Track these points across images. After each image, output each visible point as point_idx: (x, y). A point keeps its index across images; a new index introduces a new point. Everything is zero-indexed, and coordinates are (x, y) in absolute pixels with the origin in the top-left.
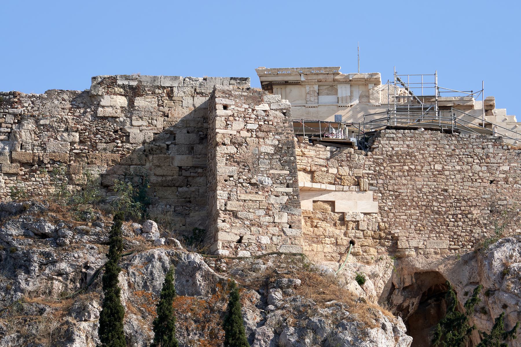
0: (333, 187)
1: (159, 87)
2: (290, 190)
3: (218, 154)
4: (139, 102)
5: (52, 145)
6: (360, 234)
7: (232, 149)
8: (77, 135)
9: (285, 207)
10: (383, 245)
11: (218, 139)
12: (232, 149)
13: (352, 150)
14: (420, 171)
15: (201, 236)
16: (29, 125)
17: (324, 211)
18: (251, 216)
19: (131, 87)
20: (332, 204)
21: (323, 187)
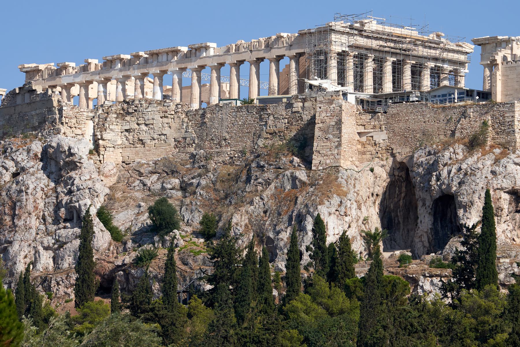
0: (372, 130)
1: (312, 97)
2: (339, 140)
3: (316, 128)
4: (306, 104)
5: (279, 125)
6: (380, 149)
7: (321, 125)
8: (286, 120)
9: (337, 147)
10: (388, 152)
11: (316, 122)
12: (321, 125)
13: (379, 114)
14: (401, 120)
15: (307, 162)
16: (271, 118)
17: (370, 140)
18: (324, 152)
19: (303, 98)
20: (372, 137)
21: (369, 131)
